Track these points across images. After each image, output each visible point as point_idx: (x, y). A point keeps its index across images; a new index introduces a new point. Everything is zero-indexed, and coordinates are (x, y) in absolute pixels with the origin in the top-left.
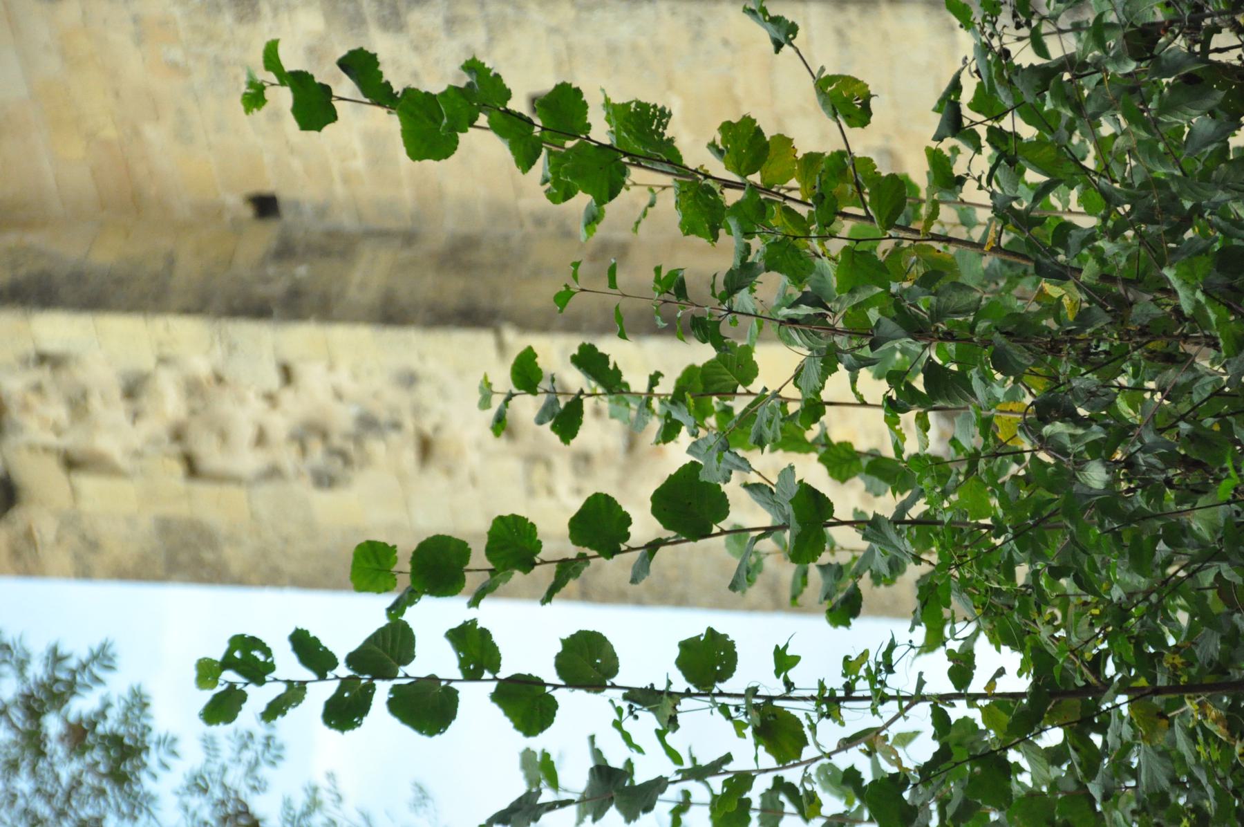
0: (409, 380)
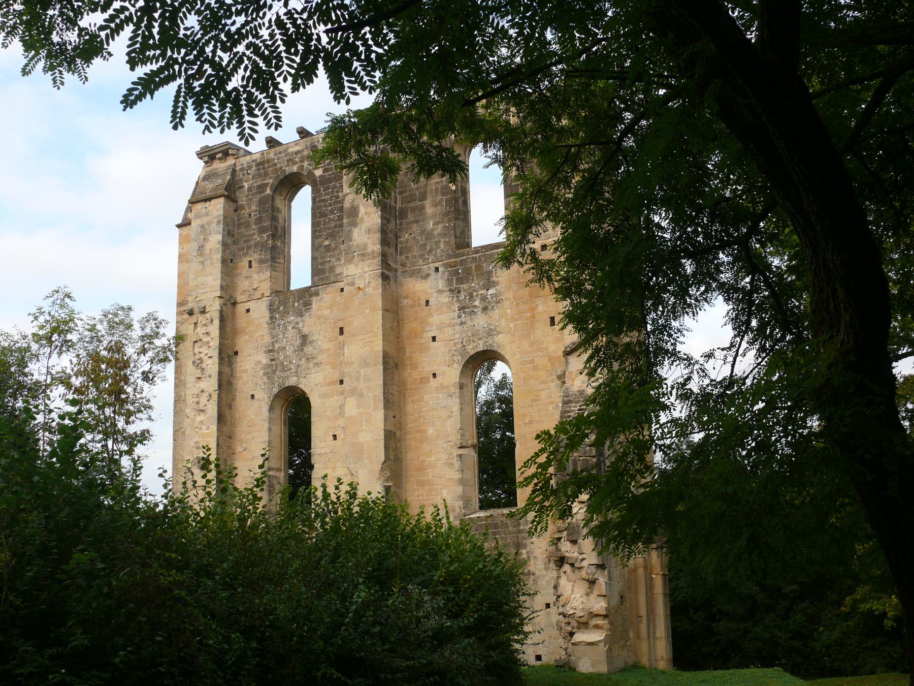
0: (210, 376)
